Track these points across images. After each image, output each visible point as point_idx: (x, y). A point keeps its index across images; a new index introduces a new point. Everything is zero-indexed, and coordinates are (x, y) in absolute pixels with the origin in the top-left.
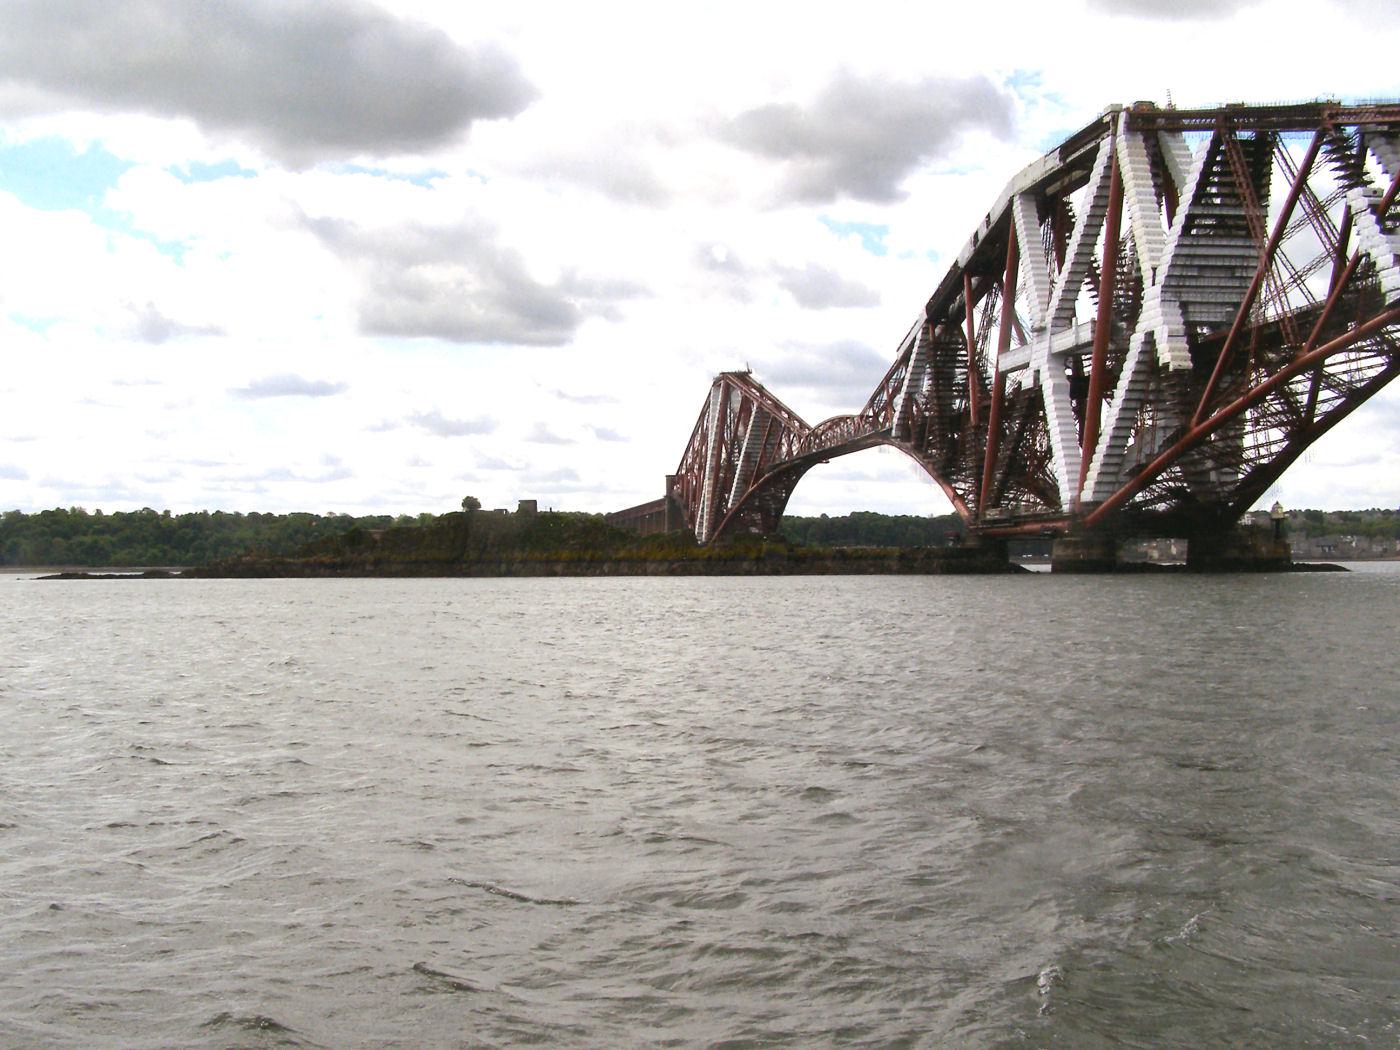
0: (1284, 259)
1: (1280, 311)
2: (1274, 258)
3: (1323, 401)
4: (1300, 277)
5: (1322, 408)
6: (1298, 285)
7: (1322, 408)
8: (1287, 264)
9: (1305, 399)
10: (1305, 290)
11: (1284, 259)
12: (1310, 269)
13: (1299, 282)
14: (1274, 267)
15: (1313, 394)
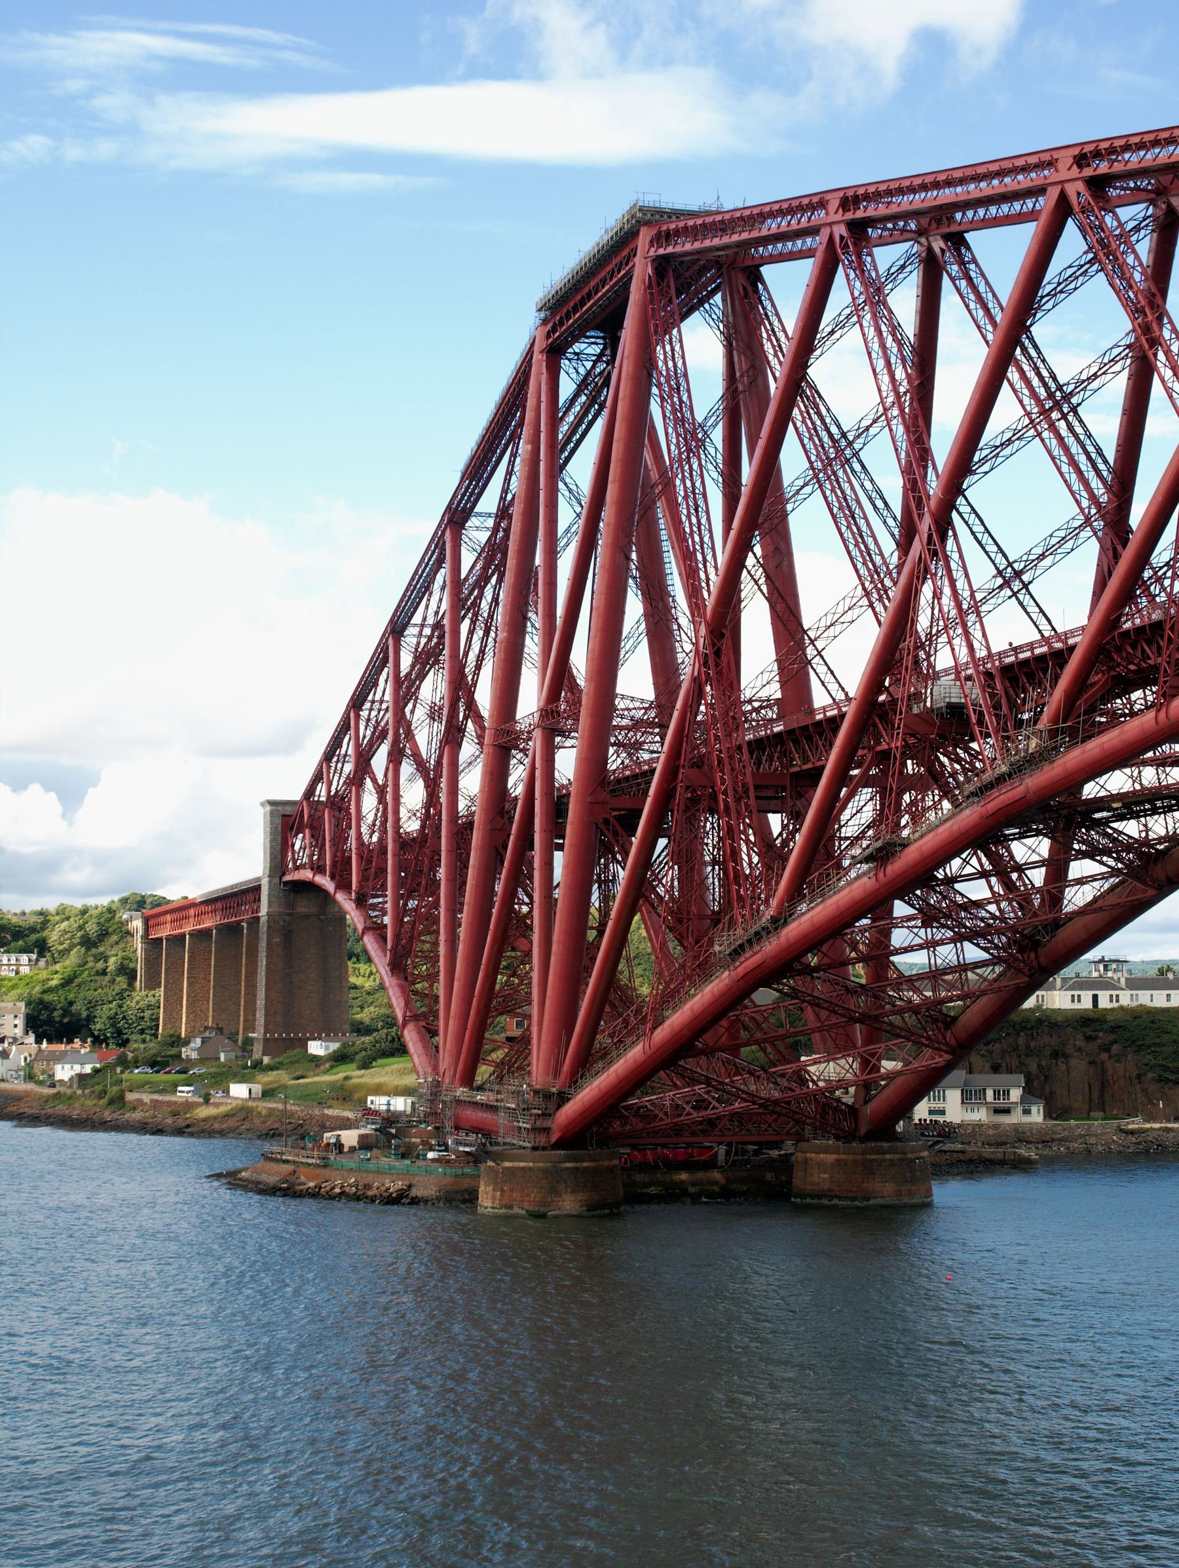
0: (978, 528)
1: (963, 654)
2: (950, 523)
3: (1081, 882)
4: (1018, 574)
5: (1077, 898)
6: (1015, 594)
7: (1077, 898)
8: (986, 539)
9: (1037, 877)
10: (1032, 608)
11: (978, 528)
12: (1042, 556)
13: (1016, 585)
14: (950, 544)
15: (1057, 868)
